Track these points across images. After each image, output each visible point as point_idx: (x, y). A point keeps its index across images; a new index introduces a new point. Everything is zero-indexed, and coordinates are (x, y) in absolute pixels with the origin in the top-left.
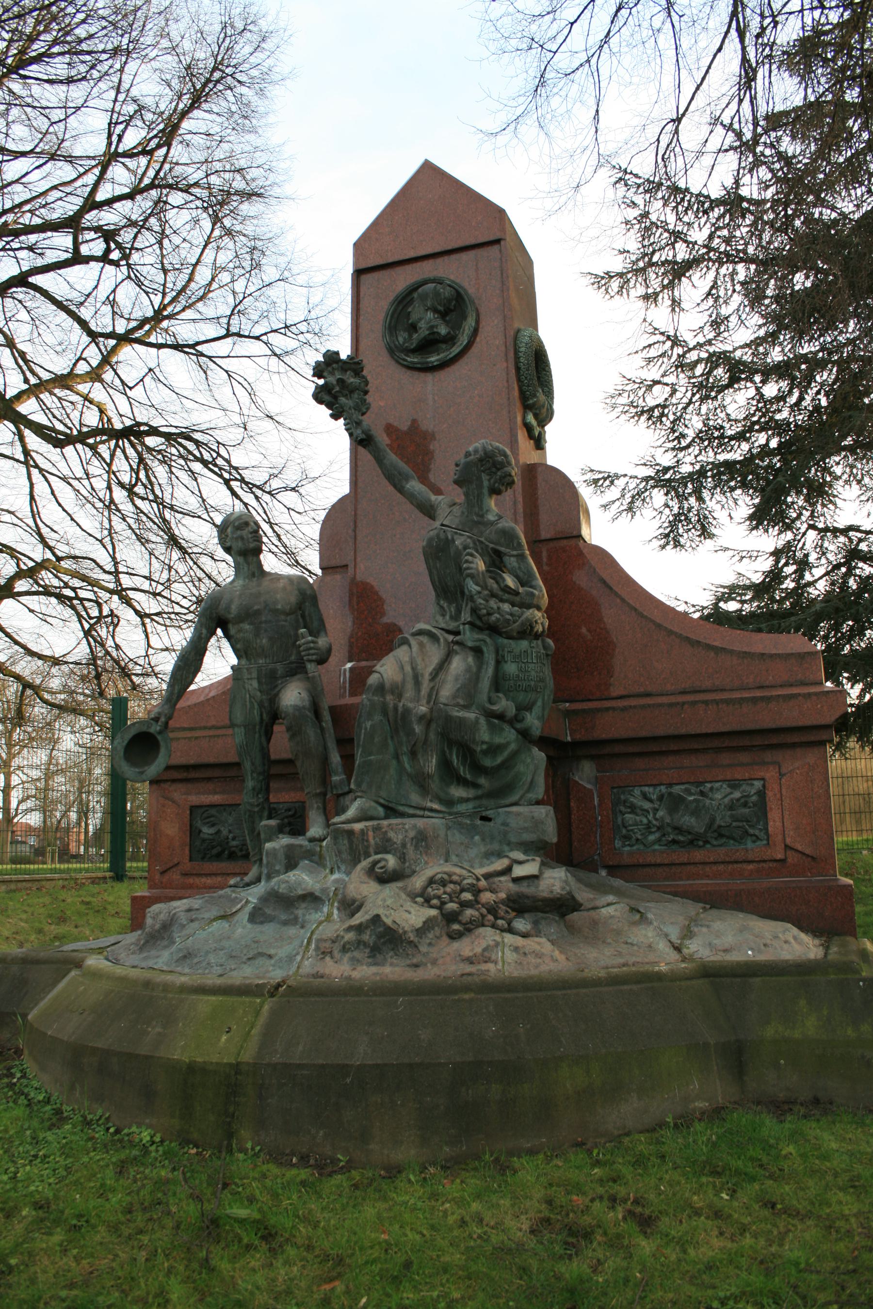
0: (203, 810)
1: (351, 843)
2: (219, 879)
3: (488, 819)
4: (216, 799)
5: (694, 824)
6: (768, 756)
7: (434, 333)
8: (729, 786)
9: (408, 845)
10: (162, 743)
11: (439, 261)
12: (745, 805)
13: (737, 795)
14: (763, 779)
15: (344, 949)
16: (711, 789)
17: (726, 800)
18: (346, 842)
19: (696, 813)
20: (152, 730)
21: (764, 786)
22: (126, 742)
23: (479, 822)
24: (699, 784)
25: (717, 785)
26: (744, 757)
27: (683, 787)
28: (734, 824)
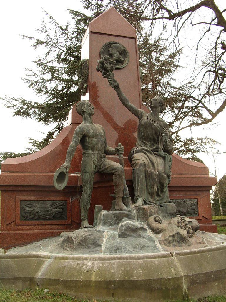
0: (25, 202)
1: (143, 212)
2: (32, 227)
3: (162, 206)
4: (32, 198)
5: (183, 210)
6: (198, 193)
7: (119, 59)
8: (190, 200)
9: (156, 213)
10: (66, 176)
11: (117, 38)
12: (194, 205)
13: (192, 203)
14: (197, 199)
15: (170, 243)
16: (186, 201)
17: (190, 204)
18: (142, 212)
19: (183, 207)
20: (65, 171)
21: (197, 201)
22: (58, 175)
23: (160, 207)
24: (183, 199)
25: (187, 200)
26: (193, 193)
27: (180, 200)
28: (192, 210)
